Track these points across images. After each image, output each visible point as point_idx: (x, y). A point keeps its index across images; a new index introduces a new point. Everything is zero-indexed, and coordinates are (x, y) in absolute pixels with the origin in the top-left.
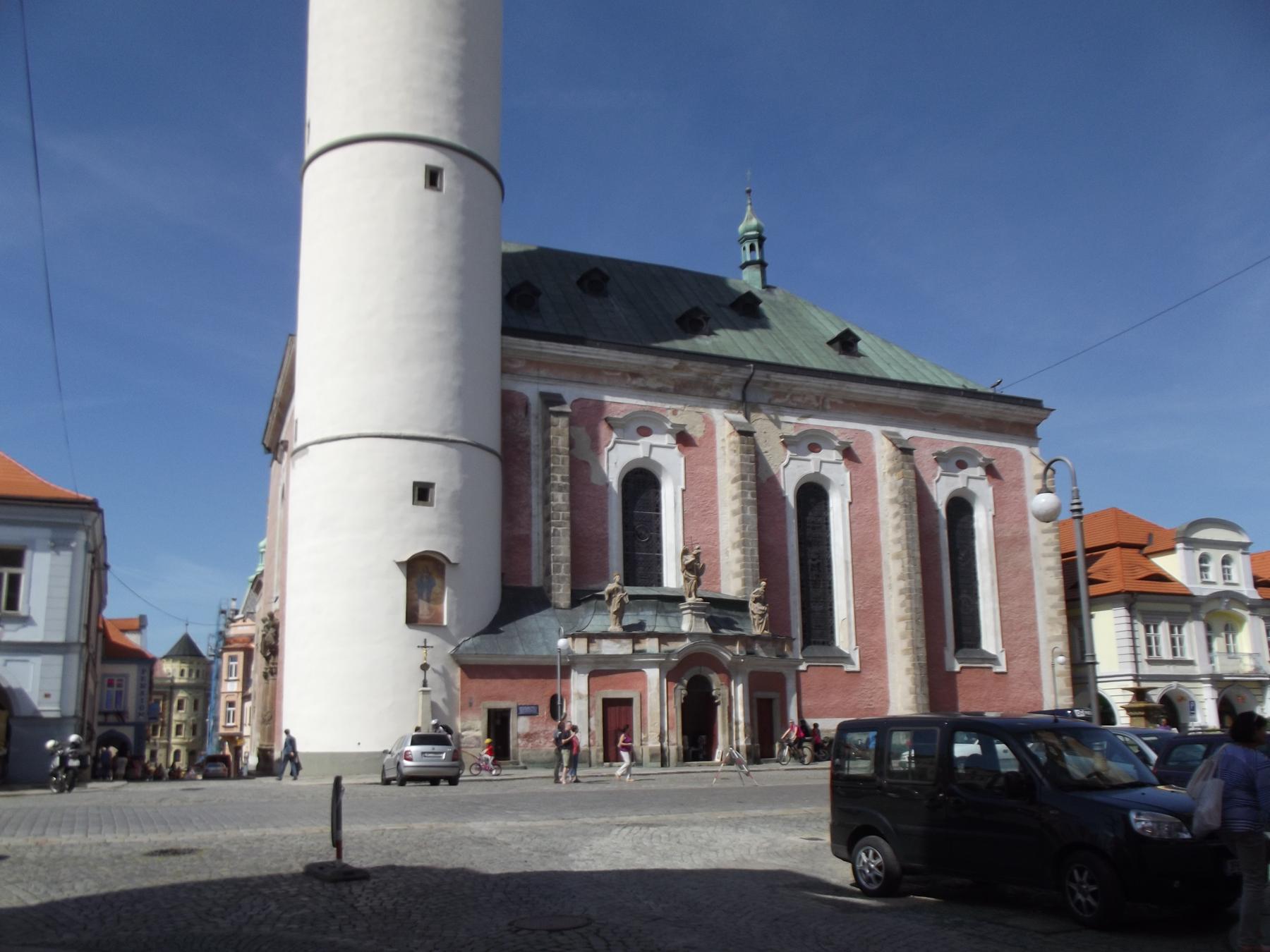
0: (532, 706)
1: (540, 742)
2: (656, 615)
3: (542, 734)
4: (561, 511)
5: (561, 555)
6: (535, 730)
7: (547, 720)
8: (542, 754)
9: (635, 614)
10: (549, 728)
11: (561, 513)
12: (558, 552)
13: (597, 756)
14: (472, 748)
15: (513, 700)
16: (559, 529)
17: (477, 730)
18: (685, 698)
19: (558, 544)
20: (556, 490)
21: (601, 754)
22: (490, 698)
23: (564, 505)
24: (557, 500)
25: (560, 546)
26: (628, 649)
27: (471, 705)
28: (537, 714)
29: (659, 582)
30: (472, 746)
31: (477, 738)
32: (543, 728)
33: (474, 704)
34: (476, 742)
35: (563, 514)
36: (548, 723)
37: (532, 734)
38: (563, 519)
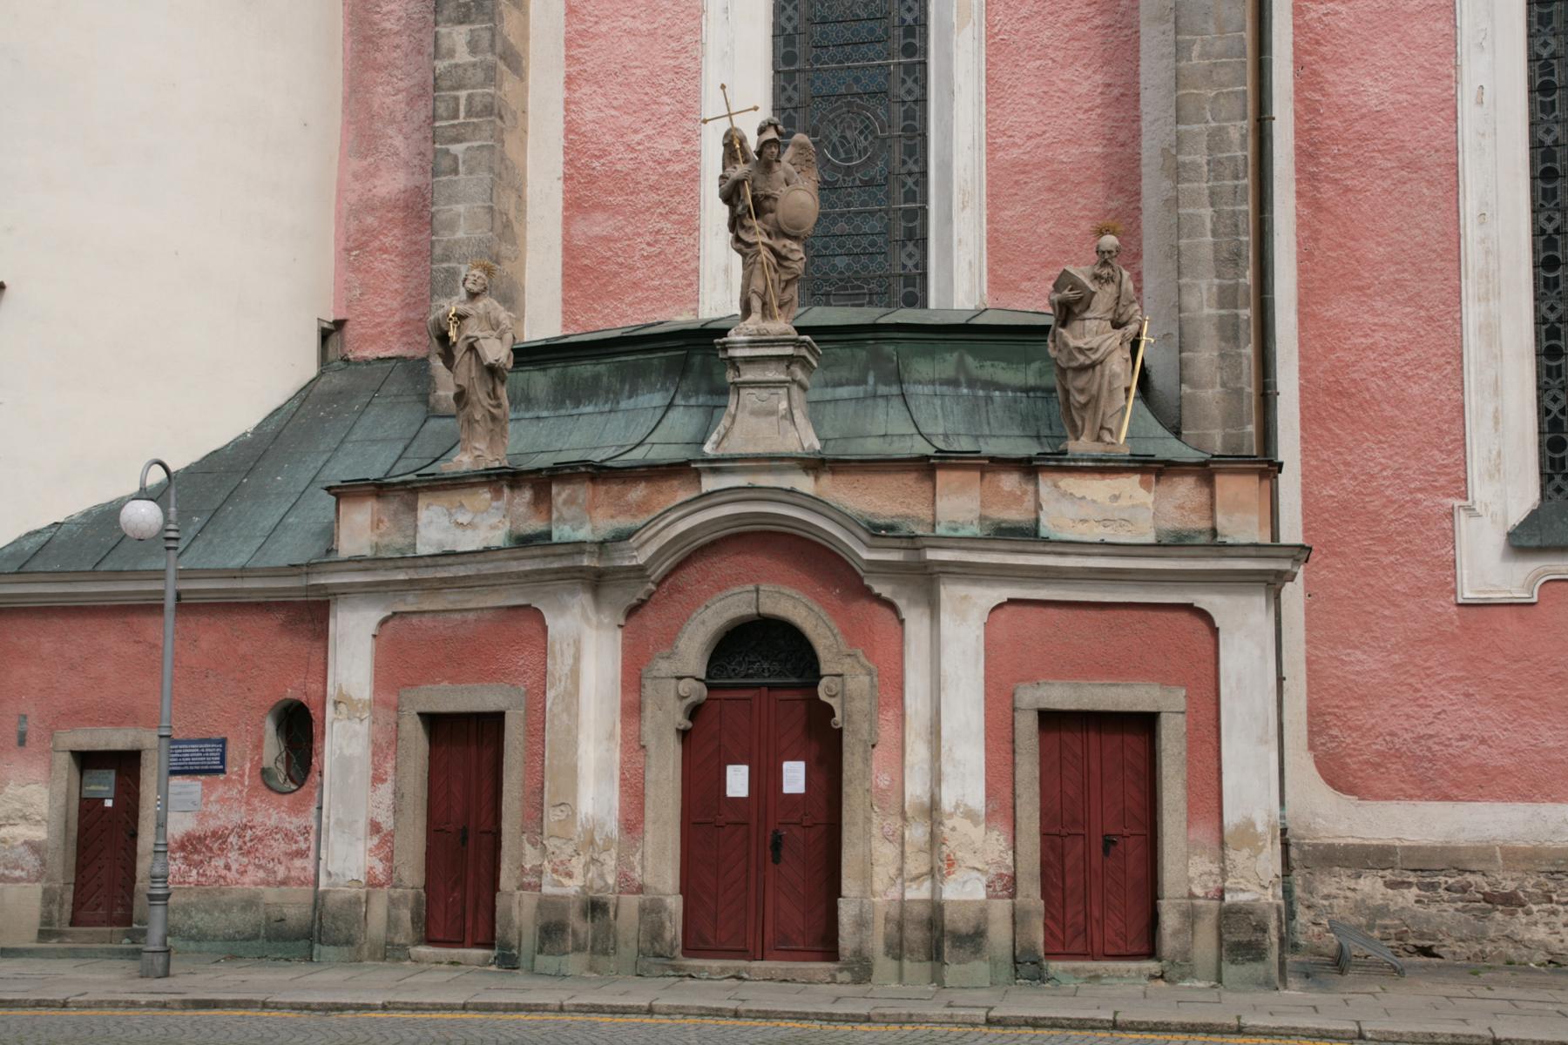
0: (208, 741)
1: (228, 867)
2: (670, 406)
3: (233, 839)
4: (460, 87)
5: (460, 234)
6: (212, 824)
7: (253, 788)
8: (227, 909)
9: (607, 407)
10: (259, 818)
11: (463, 94)
12: (451, 225)
13: (392, 923)
14: (17, 880)
15: (153, 723)
16: (457, 149)
17: (38, 823)
18: (694, 712)
19: (451, 199)
20: (449, 20)
21: (405, 915)
22: (77, 716)
23: (474, 65)
24: (451, 53)
25: (461, 208)
26: (493, 527)
27: (22, 742)
28: (223, 771)
29: (917, 299)
30: (18, 873)
31: (34, 847)
32: (237, 817)
33: (32, 737)
34: (31, 861)
35: (470, 98)
36: (256, 802)
37: (201, 839)
38: (469, 113)
